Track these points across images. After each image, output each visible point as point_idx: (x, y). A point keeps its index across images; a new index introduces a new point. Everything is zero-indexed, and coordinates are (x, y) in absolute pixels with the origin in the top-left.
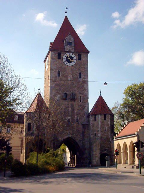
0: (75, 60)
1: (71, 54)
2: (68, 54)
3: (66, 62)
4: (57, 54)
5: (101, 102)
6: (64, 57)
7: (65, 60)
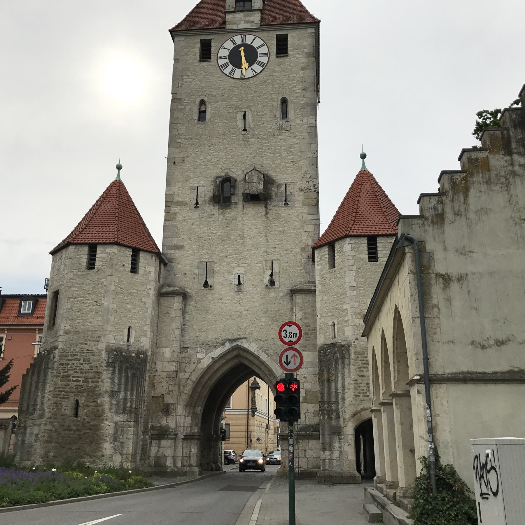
0: (263, 55)
2: (238, 39)
3: (231, 67)
4: (198, 46)
5: (365, 190)
7: (227, 60)
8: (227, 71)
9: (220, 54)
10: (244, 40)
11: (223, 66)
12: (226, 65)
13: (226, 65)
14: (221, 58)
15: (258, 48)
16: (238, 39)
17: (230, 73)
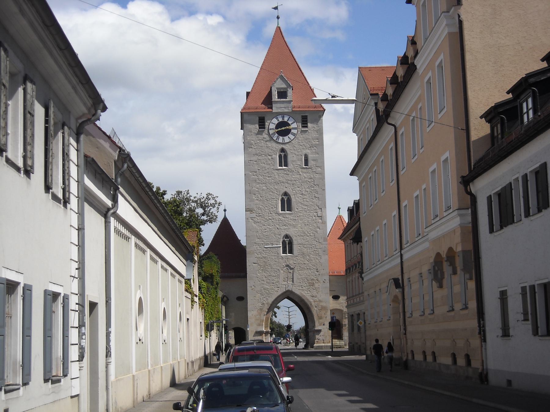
6: (272, 126)
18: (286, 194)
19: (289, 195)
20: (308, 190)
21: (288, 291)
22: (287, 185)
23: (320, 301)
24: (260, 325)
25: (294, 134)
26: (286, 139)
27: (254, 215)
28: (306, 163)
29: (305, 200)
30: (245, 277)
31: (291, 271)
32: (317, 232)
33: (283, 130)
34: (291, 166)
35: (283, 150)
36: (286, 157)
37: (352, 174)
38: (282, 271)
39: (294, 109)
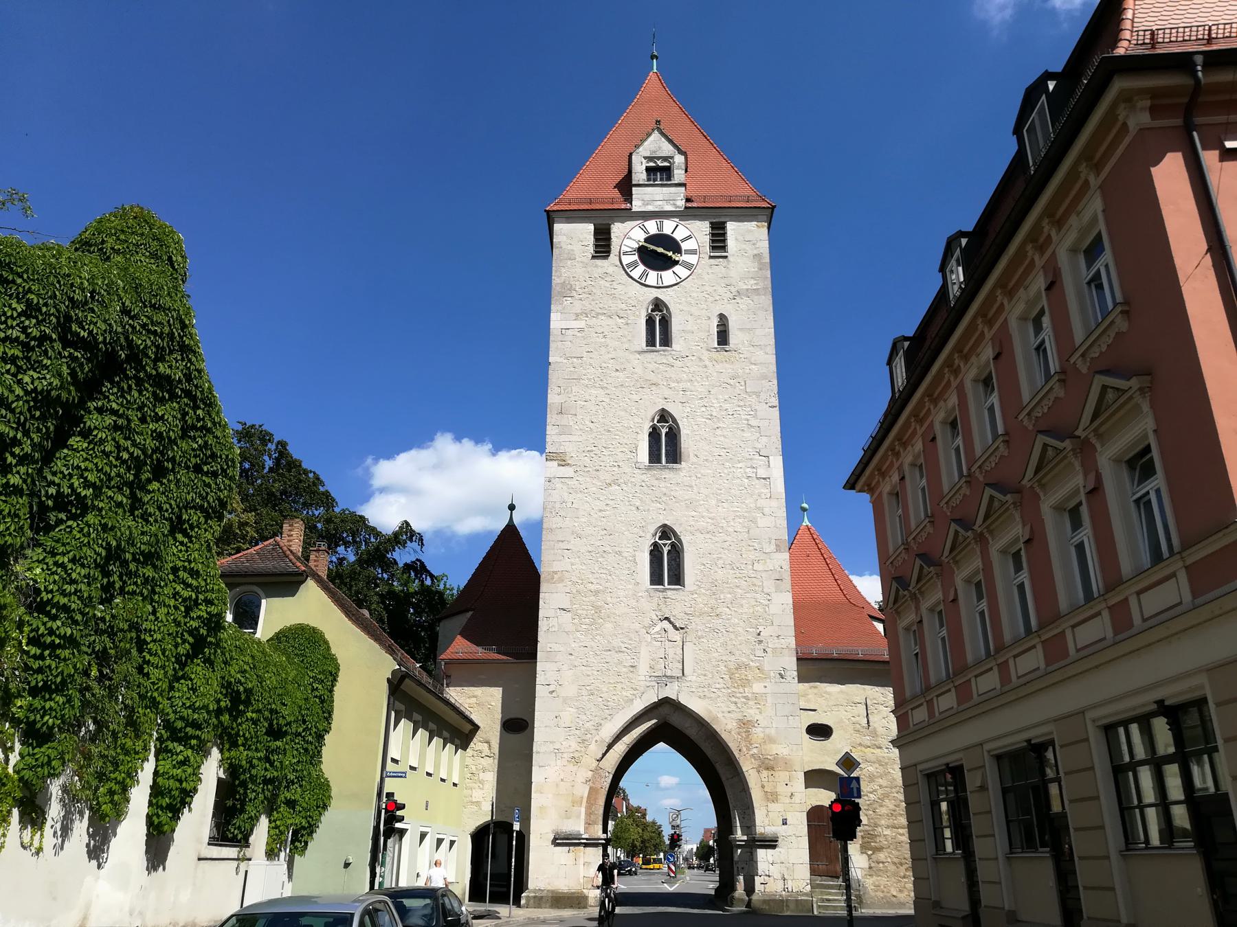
1: (668, 227)
2: (652, 227)
7: (636, 257)
8: (636, 273)
9: (624, 249)
10: (660, 228)
11: (629, 265)
12: (633, 265)
13: (633, 265)
14: (625, 253)
15: (683, 240)
16: (652, 227)
17: (641, 277)
18: (664, 416)
19: (674, 420)
20: (726, 406)
21: (666, 702)
22: (667, 393)
23: (770, 740)
24: (567, 815)
25: (688, 266)
26: (668, 276)
27: (568, 471)
28: (723, 337)
29: (719, 432)
30: (532, 656)
31: (676, 636)
32: (754, 521)
33: (658, 254)
34: (678, 343)
35: (658, 305)
36: (666, 323)
37: (851, 485)
38: (648, 637)
39: (689, 205)
